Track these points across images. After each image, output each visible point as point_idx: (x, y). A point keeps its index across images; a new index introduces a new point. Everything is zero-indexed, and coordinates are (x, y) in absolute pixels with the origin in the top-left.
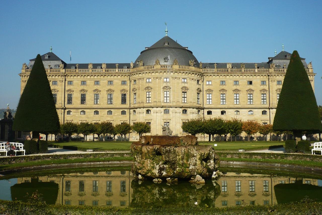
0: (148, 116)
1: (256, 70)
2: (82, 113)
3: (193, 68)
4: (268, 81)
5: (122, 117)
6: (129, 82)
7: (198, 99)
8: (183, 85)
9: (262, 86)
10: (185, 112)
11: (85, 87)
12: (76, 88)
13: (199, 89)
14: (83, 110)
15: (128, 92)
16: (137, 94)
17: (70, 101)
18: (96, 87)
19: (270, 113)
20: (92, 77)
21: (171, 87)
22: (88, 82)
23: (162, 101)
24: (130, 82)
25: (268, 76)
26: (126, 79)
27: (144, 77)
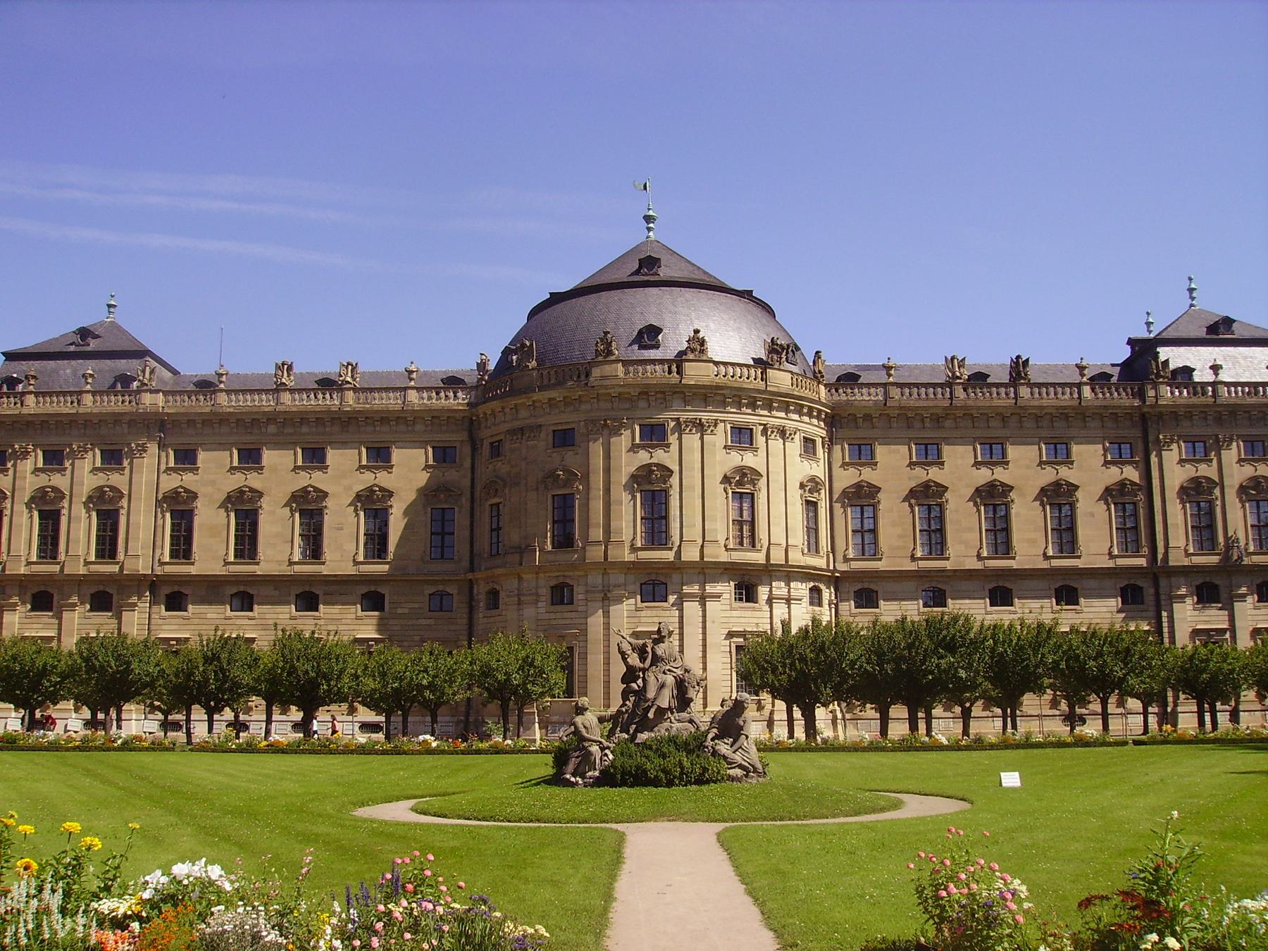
0: (559, 615)
1: (1087, 391)
2: (236, 602)
3: (781, 379)
4: (1140, 446)
5: (431, 622)
6: (467, 450)
7: (812, 530)
8: (737, 459)
9: (1114, 470)
10: (747, 593)
11: (254, 480)
12: (213, 483)
13: (813, 479)
14: (242, 589)
15: (465, 501)
16: (504, 510)
17: (182, 547)
18: (303, 480)
19: (1157, 594)
20: (288, 430)
21: (676, 468)
22: (268, 456)
23: (626, 536)
24: (474, 449)
25: (1143, 416)
26: (456, 437)
27: (540, 421)
